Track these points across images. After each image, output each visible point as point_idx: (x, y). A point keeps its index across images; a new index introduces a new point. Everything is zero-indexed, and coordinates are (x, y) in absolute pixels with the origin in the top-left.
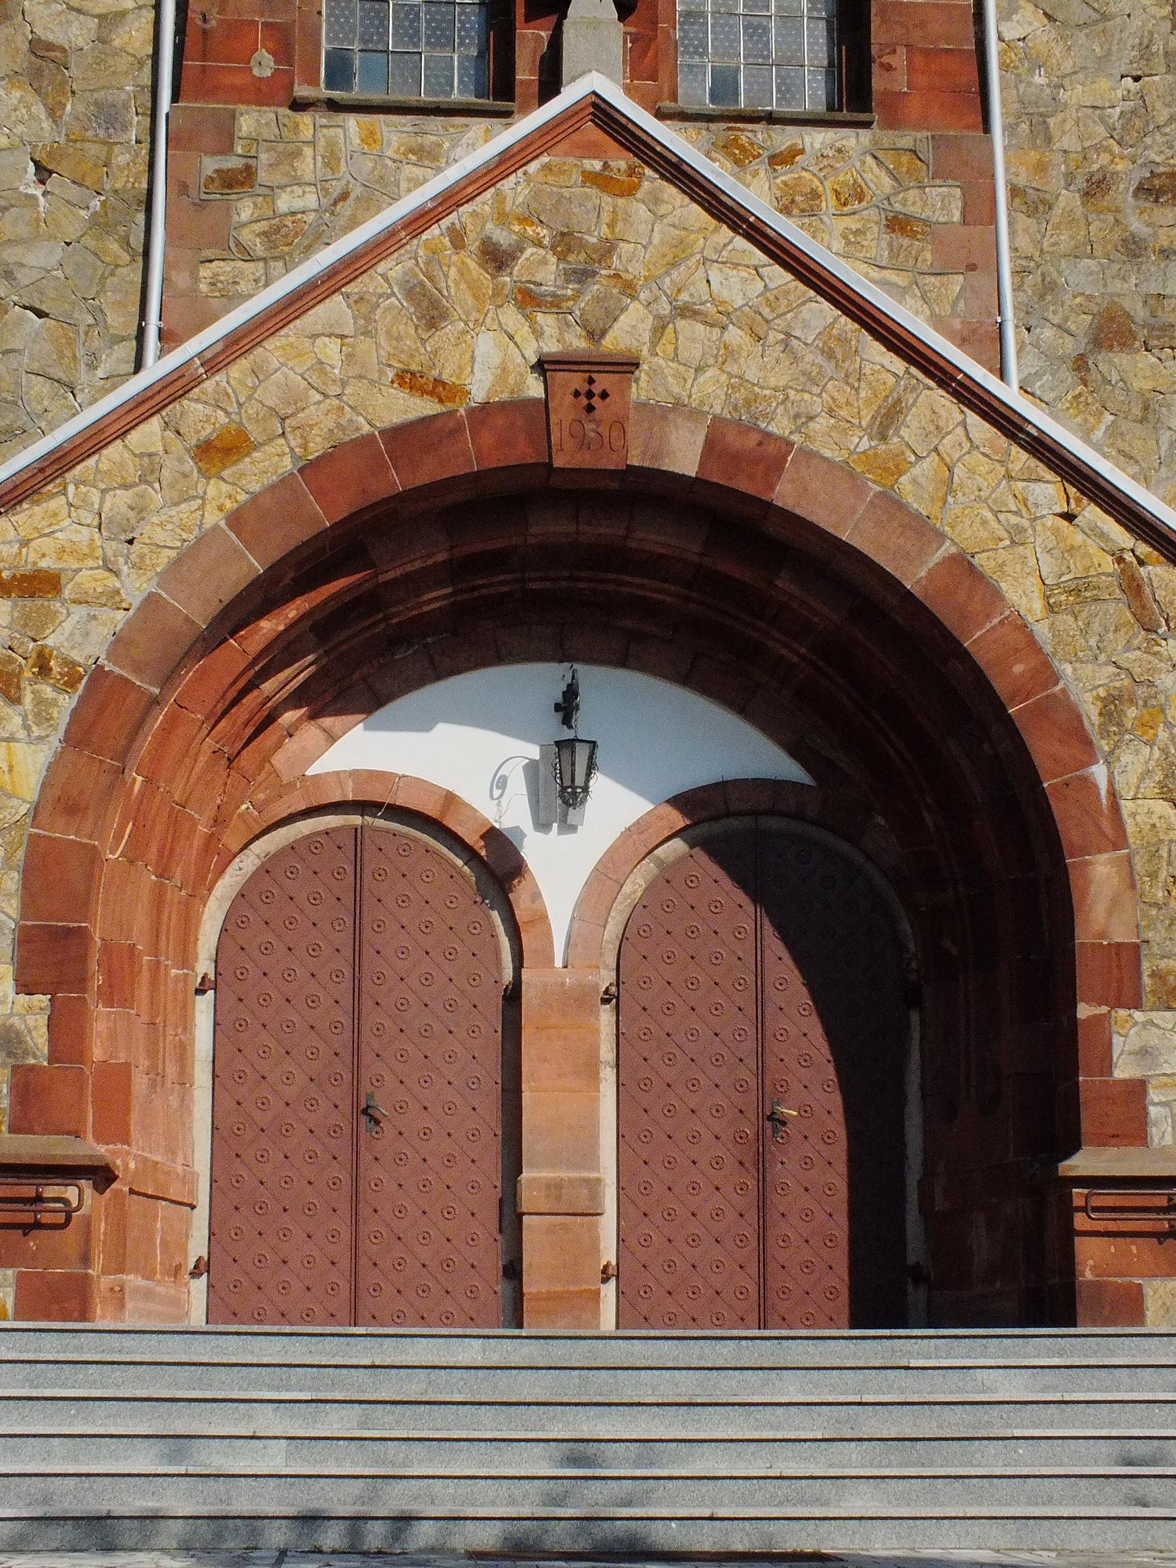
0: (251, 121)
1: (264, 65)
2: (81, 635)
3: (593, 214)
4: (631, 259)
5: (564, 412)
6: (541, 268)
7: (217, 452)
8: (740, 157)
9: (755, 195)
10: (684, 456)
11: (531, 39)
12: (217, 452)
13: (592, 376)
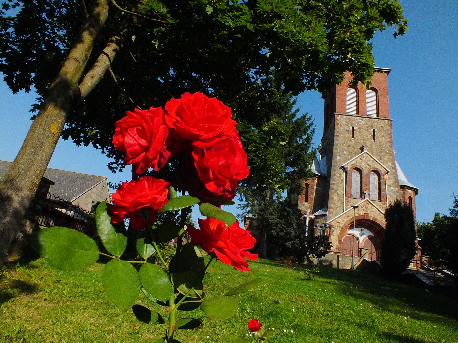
0: (349, 199)
1: (350, 196)
2: (341, 225)
3: (367, 205)
4: (369, 208)
5: (365, 216)
6: (365, 208)
7: (348, 216)
8: (374, 203)
9: (375, 205)
10: (372, 219)
11: (363, 195)
12: (348, 216)
13: (367, 214)
